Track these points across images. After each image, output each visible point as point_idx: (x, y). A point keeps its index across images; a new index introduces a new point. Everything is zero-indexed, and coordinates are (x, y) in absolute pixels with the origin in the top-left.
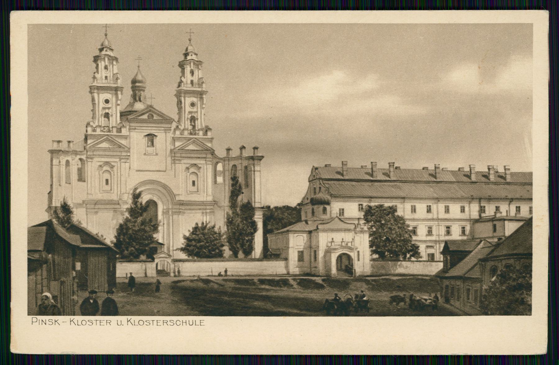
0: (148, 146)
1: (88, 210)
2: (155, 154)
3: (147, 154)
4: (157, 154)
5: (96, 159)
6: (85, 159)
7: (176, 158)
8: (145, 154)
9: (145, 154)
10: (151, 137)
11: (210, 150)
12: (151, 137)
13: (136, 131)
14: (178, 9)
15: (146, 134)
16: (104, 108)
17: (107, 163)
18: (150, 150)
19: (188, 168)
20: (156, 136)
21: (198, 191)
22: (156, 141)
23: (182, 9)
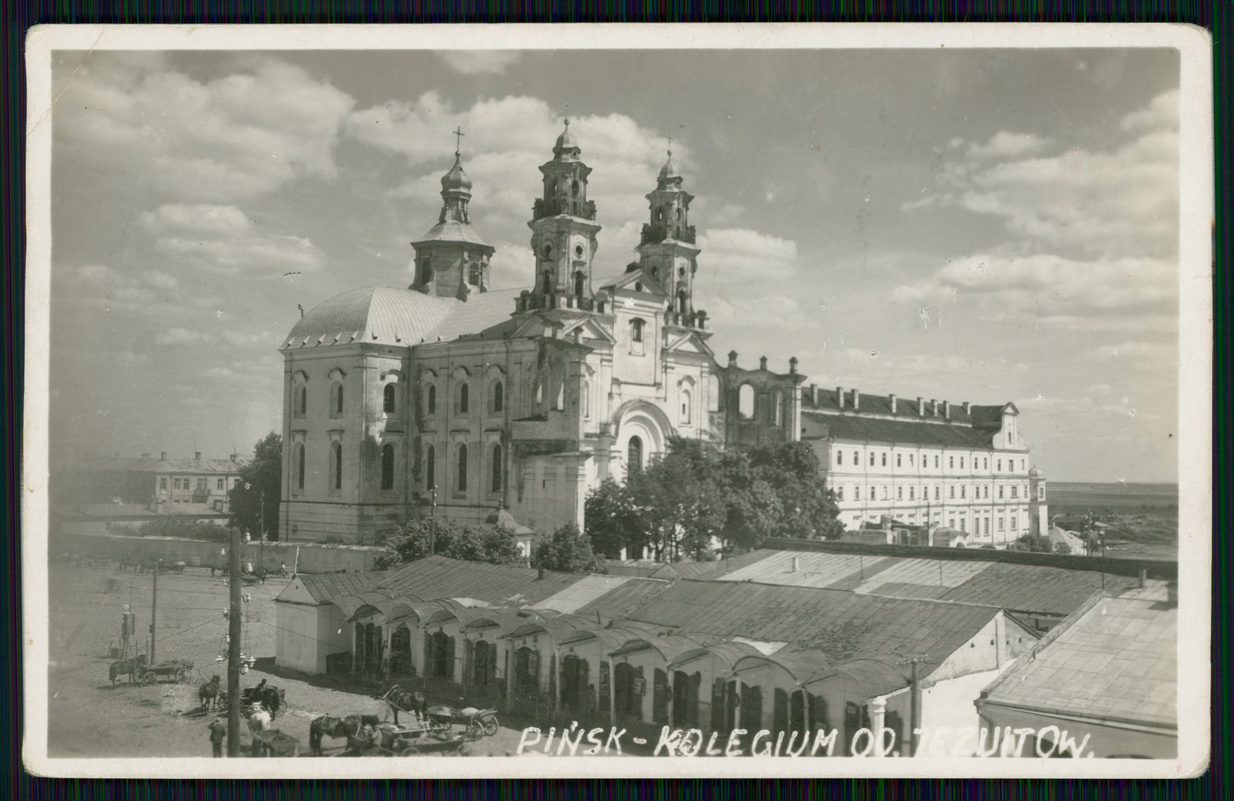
2: (641, 354)
4: (644, 355)
8: (630, 353)
9: (630, 353)
10: (638, 323)
11: (708, 354)
12: (638, 323)
13: (621, 310)
14: (262, 20)
15: (632, 317)
16: (575, 263)
18: (638, 347)
19: (680, 383)
21: (689, 423)
22: (645, 329)
23: (273, 21)
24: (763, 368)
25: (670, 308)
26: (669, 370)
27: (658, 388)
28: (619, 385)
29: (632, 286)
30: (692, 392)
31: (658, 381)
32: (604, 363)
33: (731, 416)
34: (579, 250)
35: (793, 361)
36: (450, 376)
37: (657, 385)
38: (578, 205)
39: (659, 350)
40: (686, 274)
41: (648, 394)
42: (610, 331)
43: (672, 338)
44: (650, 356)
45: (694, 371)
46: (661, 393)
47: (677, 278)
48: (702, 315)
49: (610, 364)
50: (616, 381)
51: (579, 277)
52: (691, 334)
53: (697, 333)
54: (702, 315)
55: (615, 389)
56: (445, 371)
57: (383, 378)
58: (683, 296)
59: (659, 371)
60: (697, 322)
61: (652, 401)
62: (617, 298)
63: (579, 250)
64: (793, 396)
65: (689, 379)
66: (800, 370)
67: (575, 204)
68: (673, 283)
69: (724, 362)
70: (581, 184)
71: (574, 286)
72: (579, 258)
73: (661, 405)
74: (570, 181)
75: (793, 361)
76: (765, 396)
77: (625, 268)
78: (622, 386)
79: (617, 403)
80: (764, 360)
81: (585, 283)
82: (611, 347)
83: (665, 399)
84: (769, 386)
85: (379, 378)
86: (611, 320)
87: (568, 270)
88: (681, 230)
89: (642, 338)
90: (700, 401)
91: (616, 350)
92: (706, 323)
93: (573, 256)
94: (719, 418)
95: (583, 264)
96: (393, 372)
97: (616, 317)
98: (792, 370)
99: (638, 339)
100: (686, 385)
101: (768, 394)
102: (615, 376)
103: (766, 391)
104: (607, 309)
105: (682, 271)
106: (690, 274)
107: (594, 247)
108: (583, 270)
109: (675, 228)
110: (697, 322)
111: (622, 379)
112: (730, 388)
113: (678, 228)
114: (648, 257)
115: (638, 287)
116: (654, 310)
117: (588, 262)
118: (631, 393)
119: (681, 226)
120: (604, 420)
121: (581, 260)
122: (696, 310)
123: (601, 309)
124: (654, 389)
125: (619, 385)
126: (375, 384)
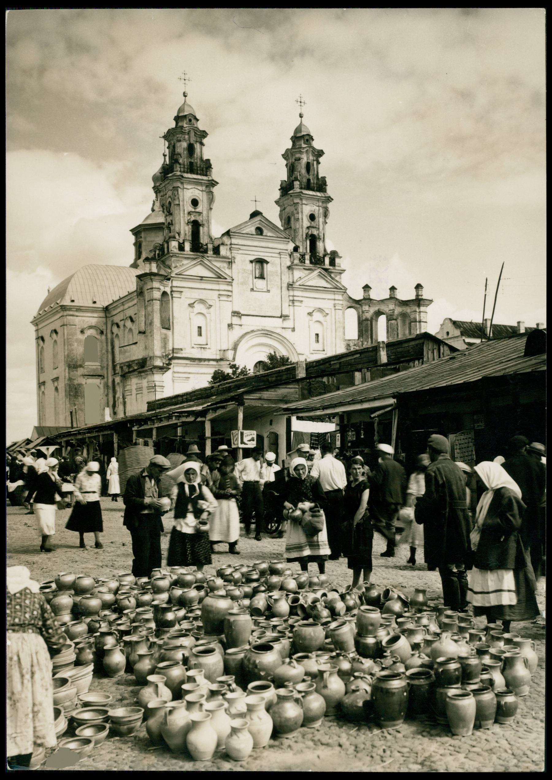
0: (256, 278)
1: (176, 375)
2: (265, 290)
3: (255, 289)
4: (268, 291)
5: (187, 293)
6: (169, 293)
7: (295, 298)
8: (252, 290)
9: (252, 290)
11: (341, 289)
13: (241, 252)
15: (252, 258)
16: (189, 213)
17: (202, 301)
18: (260, 284)
20: (267, 263)
22: (268, 268)
24: (392, 298)
25: (296, 249)
26: (296, 304)
27: (284, 320)
28: (240, 317)
29: (252, 230)
30: (324, 323)
31: (284, 313)
32: (222, 298)
33: (366, 343)
34: (195, 203)
35: (418, 287)
36: (124, 326)
37: (284, 317)
38: (195, 164)
39: (285, 285)
40: (317, 220)
41: (274, 324)
42: (228, 271)
43: (298, 274)
44: (275, 291)
45: (327, 305)
46: (289, 324)
47: (306, 223)
48: (334, 256)
49: (230, 299)
50: (236, 314)
51: (196, 226)
52: (319, 270)
53: (326, 270)
54: (334, 256)
55: (236, 320)
56: (122, 322)
57: (82, 332)
58: (313, 240)
59: (286, 304)
60: (327, 261)
61: (279, 331)
62: (234, 241)
63: (195, 203)
64: (418, 320)
65: (320, 310)
66: (425, 294)
67: (191, 164)
68: (302, 228)
69: (359, 295)
70: (197, 146)
71: (190, 233)
72: (195, 209)
73: (288, 334)
74: (185, 145)
75: (418, 287)
76: (393, 322)
77: (249, 217)
78: (243, 317)
79: (237, 332)
80: (393, 289)
81: (202, 231)
82: (230, 284)
83: (293, 330)
84: (396, 312)
85: (78, 332)
86: (230, 263)
87: (184, 220)
88: (312, 181)
89: (265, 276)
90: (334, 331)
91: (236, 287)
92: (337, 261)
93: (189, 207)
94: (355, 345)
95: (200, 213)
96: (91, 327)
97: (234, 258)
98: (417, 295)
99: (262, 277)
100: (317, 316)
101: (396, 320)
102: (236, 309)
103: (395, 317)
104: (223, 251)
105: (312, 217)
106: (321, 220)
107: (211, 200)
108: (199, 219)
109: (305, 180)
110: (327, 261)
111: (242, 312)
112: (364, 318)
113: (309, 180)
114: (284, 209)
115: (259, 231)
116: (278, 251)
117: (205, 213)
118: (249, 323)
119: (311, 177)
120: (224, 347)
121: (197, 210)
122: (329, 252)
123: (216, 251)
124: (281, 320)
125: (240, 317)
126: (75, 338)
